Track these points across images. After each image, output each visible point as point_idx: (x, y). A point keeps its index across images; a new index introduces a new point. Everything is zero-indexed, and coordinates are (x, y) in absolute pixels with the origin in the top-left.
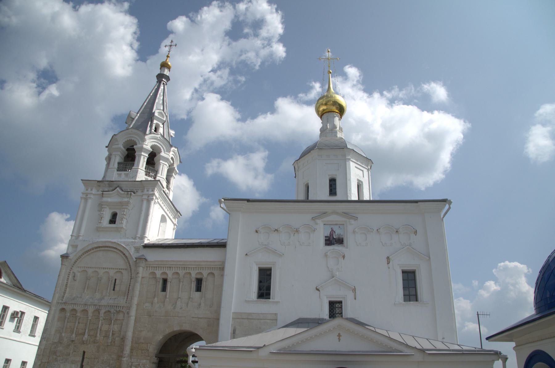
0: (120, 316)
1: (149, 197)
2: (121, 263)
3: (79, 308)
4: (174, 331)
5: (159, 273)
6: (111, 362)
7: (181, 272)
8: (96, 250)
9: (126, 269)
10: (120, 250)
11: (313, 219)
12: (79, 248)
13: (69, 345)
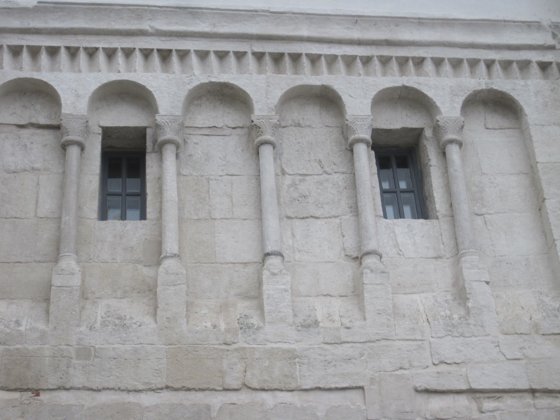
7: (264, 88)
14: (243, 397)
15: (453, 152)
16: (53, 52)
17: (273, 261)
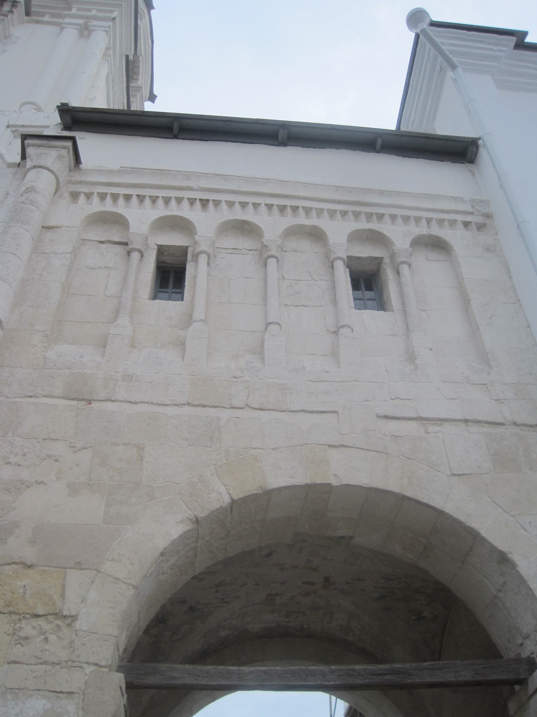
4: (268, 495)
5: (140, 219)
7: (272, 226)
14: (246, 413)
15: (404, 269)
16: (128, 198)
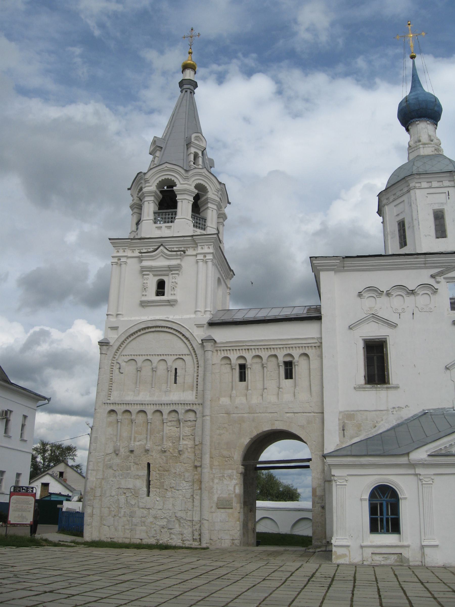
0: (191, 416)
1: (205, 256)
2: (180, 347)
3: (134, 409)
5: (233, 356)
6: (187, 474)
7: (264, 354)
8: (144, 332)
9: (188, 355)
10: (177, 331)
11: (432, 276)
12: (121, 330)
13: (128, 457)
14: (259, 414)
15: (296, 366)
17: (265, 390)
